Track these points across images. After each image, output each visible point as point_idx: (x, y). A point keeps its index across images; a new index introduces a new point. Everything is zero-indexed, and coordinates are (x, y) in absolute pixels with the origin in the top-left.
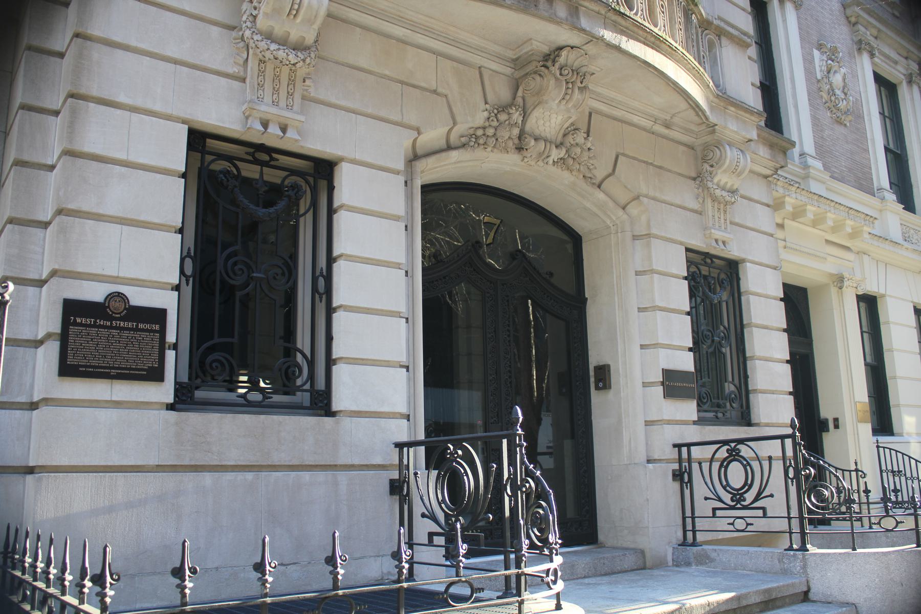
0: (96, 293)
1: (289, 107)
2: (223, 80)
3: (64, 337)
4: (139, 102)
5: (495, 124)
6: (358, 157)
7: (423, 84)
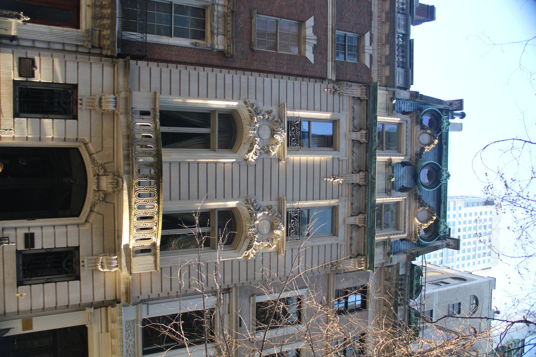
1: (86, 105)
2: (89, 91)
3: (27, 58)
4: (80, 73)
5: (98, 165)
6: (79, 124)
7: (104, 143)
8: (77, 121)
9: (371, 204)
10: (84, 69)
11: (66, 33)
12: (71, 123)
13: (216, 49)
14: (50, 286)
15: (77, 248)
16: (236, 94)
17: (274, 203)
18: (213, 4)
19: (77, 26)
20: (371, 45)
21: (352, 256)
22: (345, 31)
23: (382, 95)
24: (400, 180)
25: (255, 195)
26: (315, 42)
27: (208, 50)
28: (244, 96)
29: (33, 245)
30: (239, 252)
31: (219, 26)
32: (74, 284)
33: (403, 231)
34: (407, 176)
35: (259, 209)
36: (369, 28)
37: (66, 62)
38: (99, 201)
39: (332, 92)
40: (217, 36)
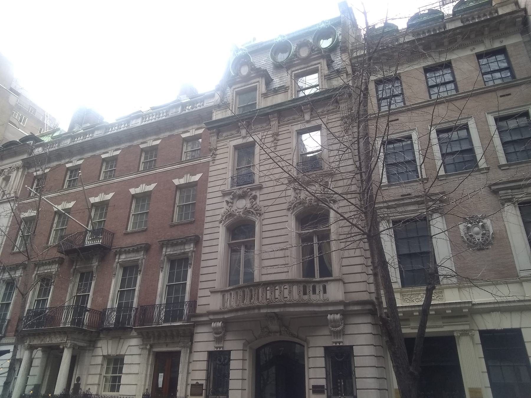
0: (194, 382)
8: (232, 350)
9: (291, 103)
10: (197, 347)
11: (182, 361)
12: (233, 356)
13: (194, 248)
14: (358, 372)
15: (326, 349)
16: (216, 230)
18: (166, 255)
19: (179, 352)
20: (189, 132)
21: (338, 107)
22: (182, 153)
23: (217, 116)
24: (282, 80)
26: (189, 175)
27: (194, 254)
28: (217, 224)
29: (323, 386)
31: (180, 249)
32: (357, 351)
33: (319, 65)
34: (281, 74)
35: (296, 198)
36: (179, 135)
37: (194, 361)
38: (288, 331)
39: (215, 156)
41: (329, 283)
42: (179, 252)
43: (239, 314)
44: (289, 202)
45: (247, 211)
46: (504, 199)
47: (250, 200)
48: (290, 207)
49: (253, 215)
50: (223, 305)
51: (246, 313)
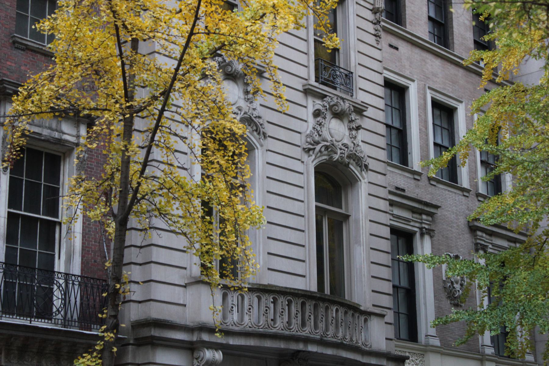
17: (313, 104)
25: (300, 133)
30: (360, 180)
35: (318, 132)
40: (64, 133)
41: (372, 317)
42: (46, 132)
43: (268, 344)
44: (307, 136)
45: (248, 120)
46: (481, 245)
47: (247, 93)
48: (312, 147)
49: (255, 133)
50: (224, 317)
51: (282, 345)
